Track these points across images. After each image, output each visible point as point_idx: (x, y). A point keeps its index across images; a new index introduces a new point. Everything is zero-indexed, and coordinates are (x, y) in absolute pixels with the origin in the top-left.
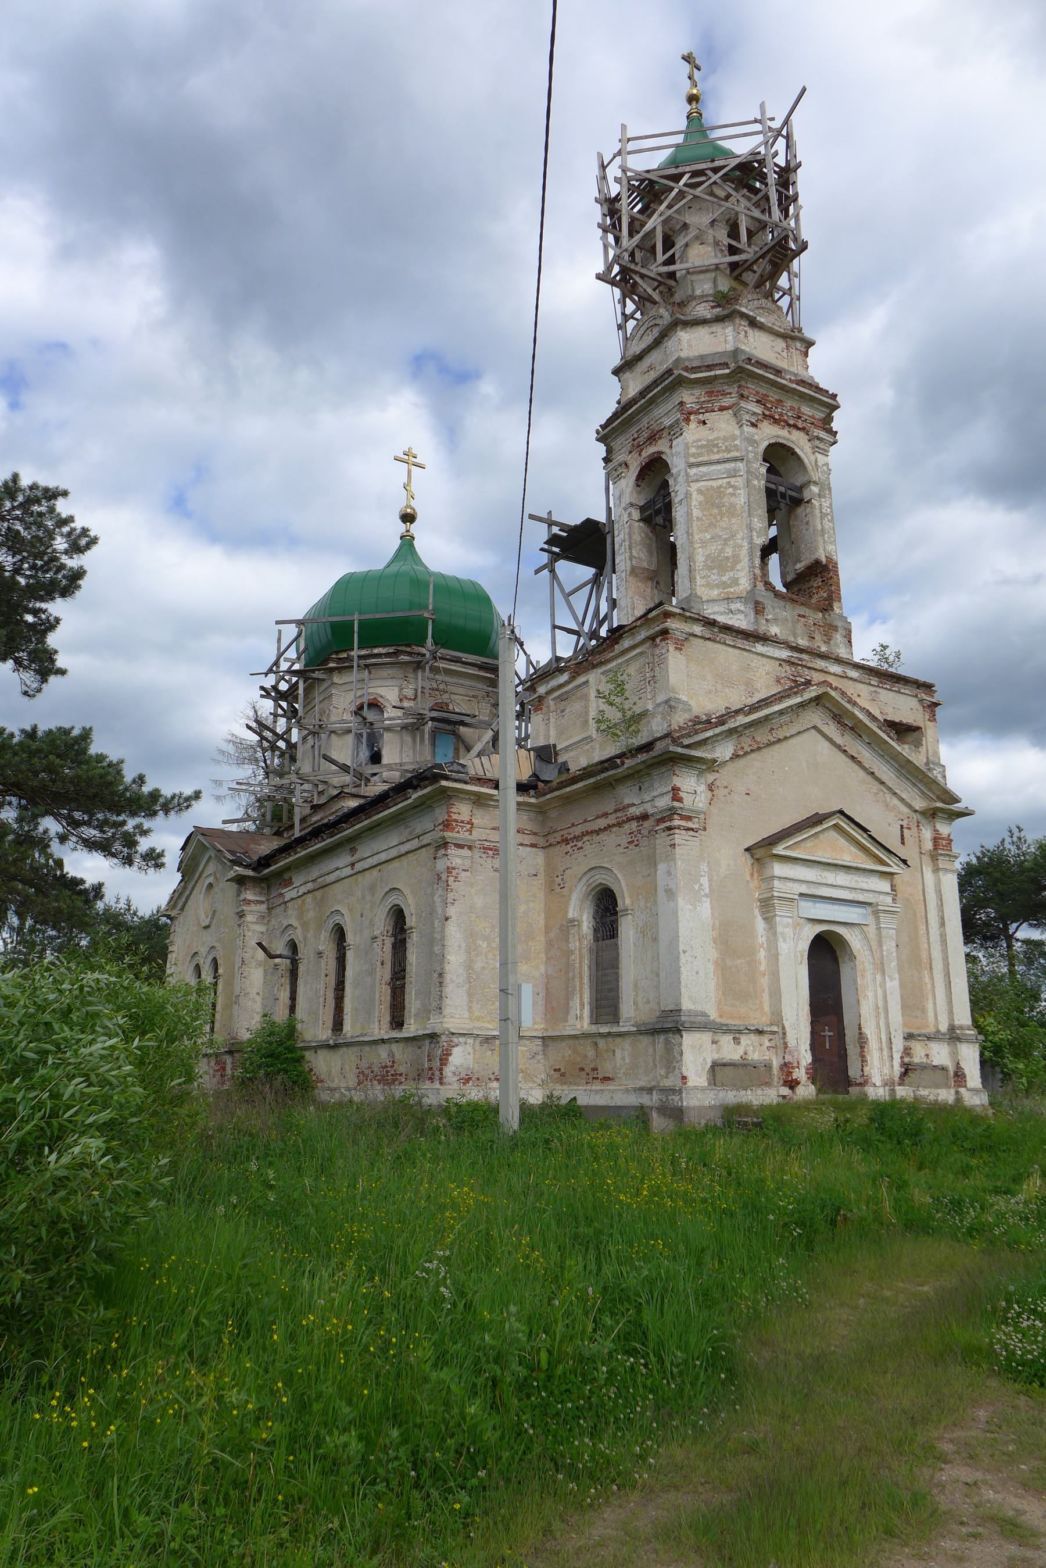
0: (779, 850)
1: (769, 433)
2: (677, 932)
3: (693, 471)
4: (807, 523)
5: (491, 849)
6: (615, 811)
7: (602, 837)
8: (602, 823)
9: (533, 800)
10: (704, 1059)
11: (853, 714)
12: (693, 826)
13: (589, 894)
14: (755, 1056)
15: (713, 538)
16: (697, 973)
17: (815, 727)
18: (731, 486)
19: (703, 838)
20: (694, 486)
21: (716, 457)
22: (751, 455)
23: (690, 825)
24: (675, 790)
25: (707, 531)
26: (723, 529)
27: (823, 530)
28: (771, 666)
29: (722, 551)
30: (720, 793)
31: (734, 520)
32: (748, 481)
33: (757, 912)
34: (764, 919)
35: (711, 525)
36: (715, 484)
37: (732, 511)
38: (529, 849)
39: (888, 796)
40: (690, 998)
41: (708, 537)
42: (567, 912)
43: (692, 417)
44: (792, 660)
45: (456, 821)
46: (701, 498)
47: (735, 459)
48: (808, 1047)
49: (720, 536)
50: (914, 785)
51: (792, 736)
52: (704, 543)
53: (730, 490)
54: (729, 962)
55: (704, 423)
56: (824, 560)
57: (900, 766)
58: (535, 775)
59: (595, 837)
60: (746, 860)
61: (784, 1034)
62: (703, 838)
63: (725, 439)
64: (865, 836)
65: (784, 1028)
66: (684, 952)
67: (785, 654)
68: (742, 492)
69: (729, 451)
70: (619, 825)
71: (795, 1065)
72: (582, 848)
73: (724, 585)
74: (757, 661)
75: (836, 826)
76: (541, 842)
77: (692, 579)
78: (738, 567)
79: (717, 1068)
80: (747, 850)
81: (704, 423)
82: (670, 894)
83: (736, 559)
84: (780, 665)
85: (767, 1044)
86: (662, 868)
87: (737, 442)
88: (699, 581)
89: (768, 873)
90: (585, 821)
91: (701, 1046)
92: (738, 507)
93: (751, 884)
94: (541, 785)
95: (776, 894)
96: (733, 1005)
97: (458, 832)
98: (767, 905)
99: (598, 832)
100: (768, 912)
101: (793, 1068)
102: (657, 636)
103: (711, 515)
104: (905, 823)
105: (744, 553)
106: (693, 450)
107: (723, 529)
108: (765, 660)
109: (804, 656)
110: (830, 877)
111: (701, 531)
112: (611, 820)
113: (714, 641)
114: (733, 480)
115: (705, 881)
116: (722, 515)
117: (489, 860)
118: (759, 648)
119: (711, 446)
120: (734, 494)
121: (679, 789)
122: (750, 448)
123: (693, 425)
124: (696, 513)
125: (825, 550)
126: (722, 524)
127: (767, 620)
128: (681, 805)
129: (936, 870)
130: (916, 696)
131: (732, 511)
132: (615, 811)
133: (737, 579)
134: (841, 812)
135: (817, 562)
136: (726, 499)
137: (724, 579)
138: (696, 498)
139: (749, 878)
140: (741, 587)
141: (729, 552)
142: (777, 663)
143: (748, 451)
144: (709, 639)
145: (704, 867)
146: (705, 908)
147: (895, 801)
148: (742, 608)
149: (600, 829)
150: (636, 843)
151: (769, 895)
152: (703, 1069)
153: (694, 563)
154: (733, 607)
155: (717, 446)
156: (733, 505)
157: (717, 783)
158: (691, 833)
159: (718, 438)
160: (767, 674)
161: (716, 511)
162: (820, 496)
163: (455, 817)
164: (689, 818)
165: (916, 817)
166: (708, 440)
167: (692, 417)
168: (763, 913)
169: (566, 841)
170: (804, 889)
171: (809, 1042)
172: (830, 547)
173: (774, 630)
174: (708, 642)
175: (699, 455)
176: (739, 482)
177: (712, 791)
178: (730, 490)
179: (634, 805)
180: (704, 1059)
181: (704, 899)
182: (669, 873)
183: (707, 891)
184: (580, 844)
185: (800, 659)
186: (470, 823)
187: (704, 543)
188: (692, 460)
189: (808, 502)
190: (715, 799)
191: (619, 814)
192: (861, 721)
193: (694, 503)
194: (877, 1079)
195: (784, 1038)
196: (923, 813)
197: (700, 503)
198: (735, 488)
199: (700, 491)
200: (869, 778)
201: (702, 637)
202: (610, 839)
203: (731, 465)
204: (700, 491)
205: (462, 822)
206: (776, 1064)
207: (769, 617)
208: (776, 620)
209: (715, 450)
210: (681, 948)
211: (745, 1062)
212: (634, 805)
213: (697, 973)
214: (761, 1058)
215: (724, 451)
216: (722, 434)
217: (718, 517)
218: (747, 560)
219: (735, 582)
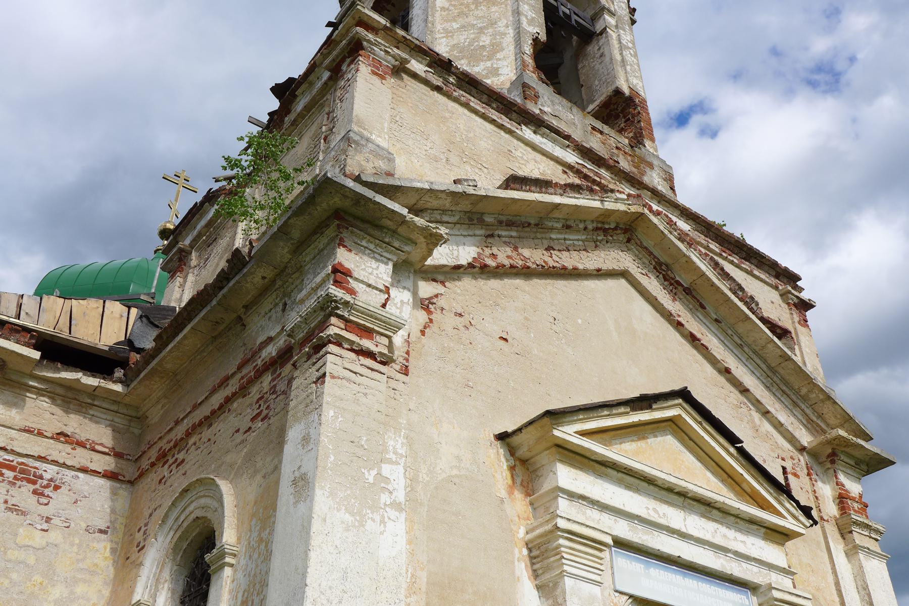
0: (568, 432)
2: (304, 575)
4: (602, 55)
5: (12, 468)
6: (240, 368)
7: (216, 426)
8: (217, 400)
9: (118, 388)
11: (689, 261)
12: (373, 348)
13: (175, 548)
15: (463, 27)
17: (624, 274)
19: (400, 386)
23: (367, 344)
25: (455, 21)
26: (478, 18)
27: (623, 61)
30: (445, 321)
31: (494, 9)
33: (522, 570)
34: (539, 588)
38: (101, 481)
39: (756, 416)
42: (132, 592)
44: (585, 170)
49: (474, 25)
50: (795, 404)
56: (627, 91)
57: (769, 367)
58: (129, 342)
59: (207, 433)
60: (497, 461)
62: (400, 386)
64: (732, 450)
67: (572, 158)
70: (243, 391)
72: (183, 461)
74: (522, 151)
75: (673, 425)
76: (130, 472)
78: (498, 56)
80: (502, 437)
82: (303, 484)
83: (496, 48)
84: (565, 172)
86: (294, 434)
89: (546, 486)
90: (196, 407)
93: (507, 506)
94: (135, 357)
95: (562, 524)
98: (542, 554)
99: (208, 421)
100: (547, 569)
102: (343, 61)
107: (478, 18)
108: (539, 157)
109: (603, 172)
110: (675, 517)
112: (233, 386)
113: (449, 96)
115: (396, 474)
118: (527, 133)
125: (627, 80)
126: (476, 12)
128: (348, 298)
129: (852, 551)
130: (776, 288)
132: (240, 368)
133: (497, 69)
134: (684, 395)
135: (618, 92)
139: (503, 493)
140: (502, 78)
141: (485, 40)
142: (560, 168)
144: (438, 89)
145: (396, 444)
146: (392, 538)
147: (767, 427)
149: (213, 412)
150: (265, 412)
151: (549, 527)
157: (441, 302)
158: (369, 362)
162: (617, 27)
164: (367, 332)
165: (803, 459)
168: (536, 575)
169: (163, 456)
170: (624, 530)
172: (635, 81)
174: (436, 94)
177: (429, 312)
179: (270, 339)
181: (393, 513)
182: (306, 439)
183: (400, 496)
184: (180, 456)
185: (597, 174)
187: (449, 33)
189: (601, 33)
190: (434, 327)
191: (245, 371)
192: (704, 274)
196: (812, 453)
200: (721, 380)
201: (426, 82)
202: (224, 427)
212: (270, 339)
217: (473, 7)
218: (512, 48)
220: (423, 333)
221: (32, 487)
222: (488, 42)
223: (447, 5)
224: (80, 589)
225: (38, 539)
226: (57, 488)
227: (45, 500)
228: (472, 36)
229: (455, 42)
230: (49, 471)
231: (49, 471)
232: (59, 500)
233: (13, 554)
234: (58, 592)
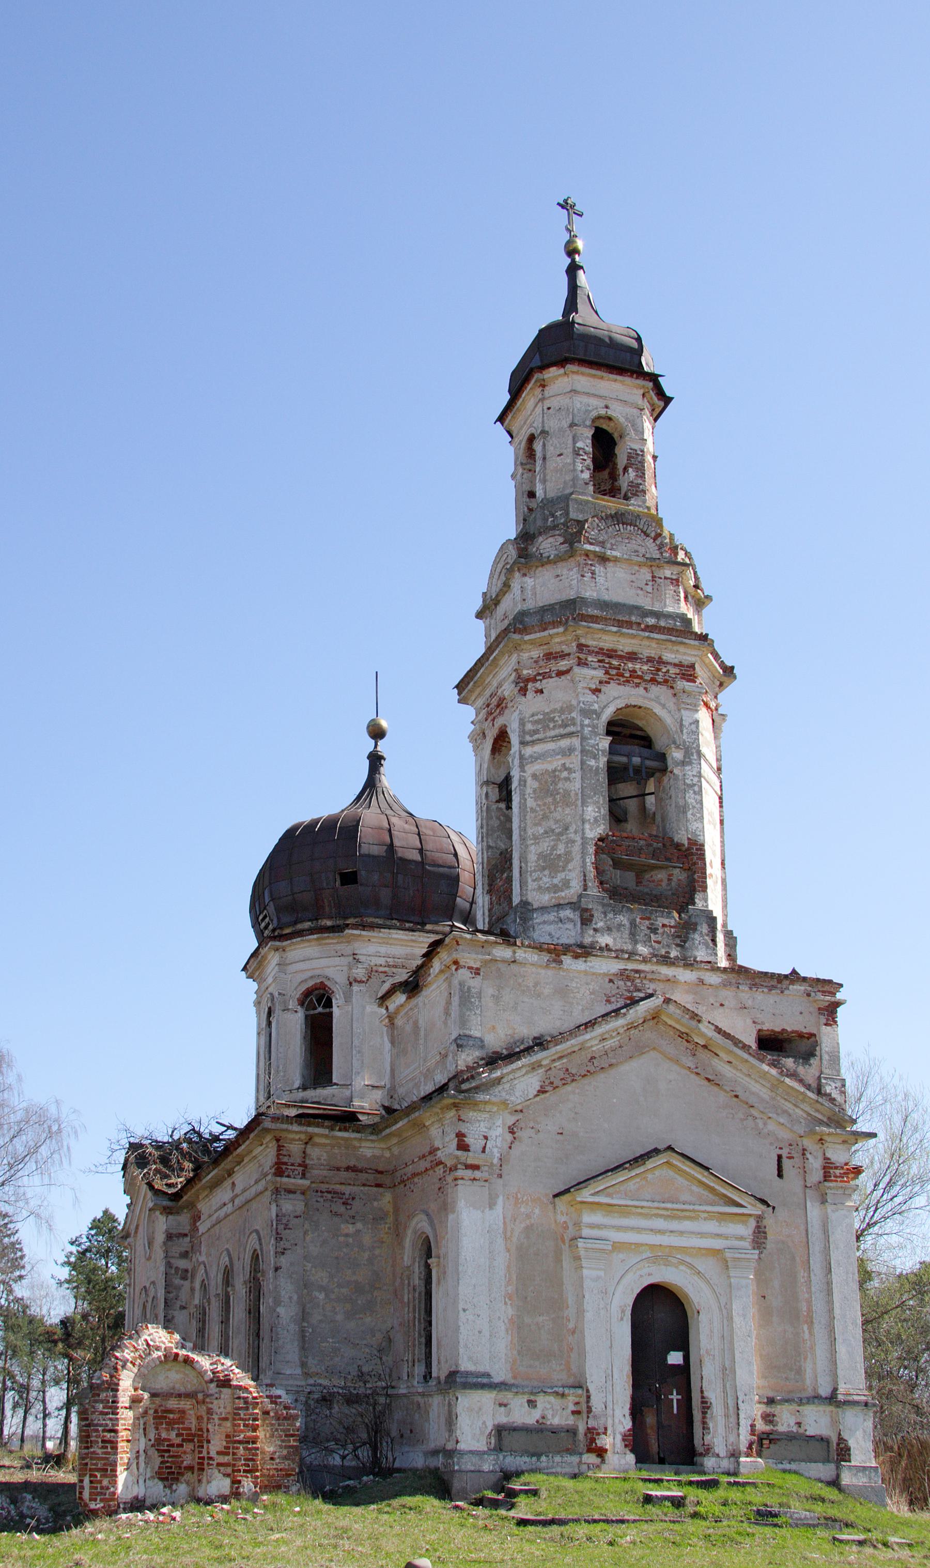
3: (528, 751)
10: (484, 1423)
14: (556, 1420)
15: (546, 832)
16: (480, 1332)
18: (566, 769)
20: (531, 769)
21: (553, 733)
22: (587, 730)
25: (541, 825)
26: (557, 822)
29: (554, 848)
31: (567, 811)
32: (583, 763)
35: (545, 817)
36: (550, 767)
40: (470, 1358)
41: (542, 831)
43: (530, 685)
46: (536, 785)
47: (570, 735)
48: (627, 1411)
52: (536, 838)
53: (565, 774)
54: (527, 1320)
55: (541, 692)
61: (588, 1397)
63: (562, 711)
65: (588, 1391)
66: (464, 1310)
68: (577, 775)
69: (566, 726)
71: (601, 1430)
73: (555, 889)
77: (523, 884)
78: (570, 866)
79: (504, 1433)
81: (541, 692)
85: (572, 1407)
87: (574, 715)
88: (531, 885)
91: (480, 1409)
96: (530, 1366)
101: (598, 1434)
103: (545, 804)
105: (576, 848)
106: (529, 727)
107: (557, 822)
111: (536, 825)
114: (567, 761)
117: (327, 1204)
119: (546, 720)
120: (567, 779)
121: (464, 1135)
122: (587, 722)
123: (530, 694)
124: (530, 803)
126: (555, 814)
127: (595, 930)
136: (560, 785)
137: (556, 881)
138: (532, 784)
140: (572, 891)
141: (561, 849)
143: (582, 726)
148: (571, 916)
152: (482, 1433)
153: (526, 863)
155: (552, 720)
156: (567, 793)
159: (553, 711)
160: (591, 993)
161: (550, 800)
163: (285, 1159)
166: (545, 714)
167: (530, 685)
171: (628, 1406)
173: (605, 940)
175: (536, 732)
177: (512, 1132)
178: (565, 774)
180: (484, 1423)
186: (304, 1165)
188: (528, 738)
193: (529, 790)
194: (720, 1448)
195: (588, 1402)
197: (535, 791)
198: (570, 770)
199: (534, 776)
203: (565, 743)
204: (534, 776)
205: (293, 1165)
206: (582, 1429)
207: (600, 924)
209: (551, 725)
210: (461, 1306)
211: (543, 1426)
213: (480, 1332)
214: (563, 1423)
215: (560, 726)
216: (558, 706)
217: (552, 807)
219: (566, 884)
220: (510, 1148)
221: (341, 1201)
222: (562, 851)
224: (377, 1252)
225: (351, 1229)
226: (353, 1198)
227: (349, 1207)
228: (552, 843)
229: (540, 850)
230: (347, 1190)
231: (347, 1190)
232: (356, 1204)
234: (366, 1255)
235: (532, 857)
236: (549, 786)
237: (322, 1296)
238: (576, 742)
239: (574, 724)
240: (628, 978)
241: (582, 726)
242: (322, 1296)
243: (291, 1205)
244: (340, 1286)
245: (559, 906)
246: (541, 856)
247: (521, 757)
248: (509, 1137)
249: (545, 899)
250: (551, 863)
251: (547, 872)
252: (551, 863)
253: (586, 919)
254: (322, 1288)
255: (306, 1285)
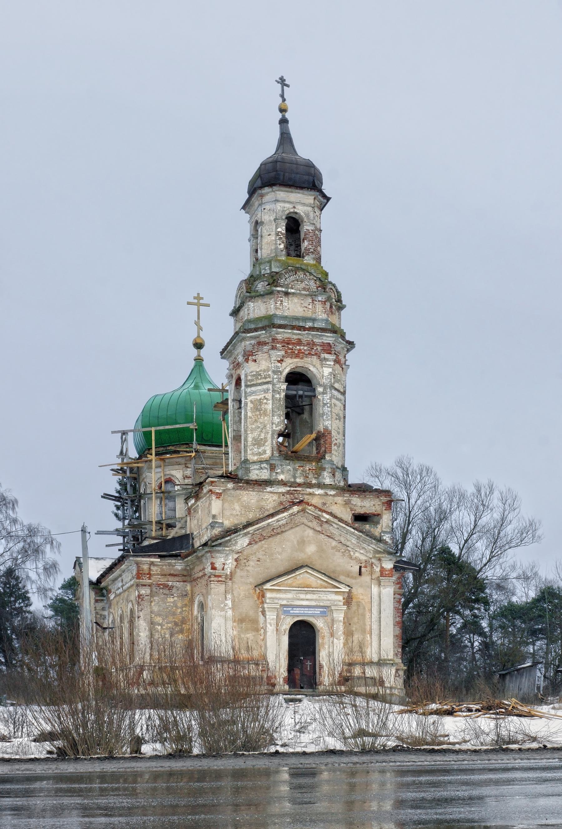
1: (288, 366)
3: (249, 390)
17: (303, 524)
18: (266, 399)
20: (249, 398)
22: (275, 381)
23: (220, 579)
24: (212, 564)
26: (261, 423)
28: (275, 497)
29: (259, 435)
31: (266, 418)
32: (273, 396)
35: (256, 421)
36: (258, 397)
37: (265, 414)
45: (141, 574)
46: (252, 406)
51: (287, 530)
53: (265, 401)
63: (264, 371)
69: (265, 378)
73: (260, 454)
74: (267, 496)
77: (246, 451)
78: (266, 444)
83: (265, 440)
87: (270, 373)
92: (268, 410)
97: (143, 579)
104: (363, 565)
106: (249, 378)
107: (261, 423)
111: (251, 424)
114: (266, 395)
116: (261, 415)
117: (161, 591)
119: (257, 375)
120: (266, 403)
122: (275, 377)
124: (249, 414)
131: (265, 414)
134: (307, 566)
136: (263, 406)
137: (260, 450)
138: (250, 405)
140: (267, 455)
143: (273, 378)
148: (266, 467)
153: (247, 442)
154: (262, 466)
155: (260, 375)
159: (261, 371)
161: (258, 413)
166: (257, 372)
173: (281, 477)
175: (252, 380)
176: (269, 396)
188: (249, 383)
190: (239, 565)
193: (249, 408)
197: (251, 408)
199: (251, 402)
203: (265, 387)
205: (144, 574)
207: (279, 471)
208: (282, 472)
215: (263, 378)
218: (270, 440)
219: (265, 452)
223: (251, 415)
233: (168, 604)
235: (250, 439)
236: (258, 406)
237: (159, 628)
238: (270, 386)
239: (270, 377)
240: (292, 494)
241: (273, 378)
242: (159, 628)
243: (144, 591)
244: (167, 623)
245: (261, 462)
246: (253, 438)
247: (246, 393)
248: (235, 563)
249: (255, 458)
250: (258, 443)
251: (256, 446)
252: (258, 443)
253: (272, 468)
254: (159, 624)
255: (152, 623)
